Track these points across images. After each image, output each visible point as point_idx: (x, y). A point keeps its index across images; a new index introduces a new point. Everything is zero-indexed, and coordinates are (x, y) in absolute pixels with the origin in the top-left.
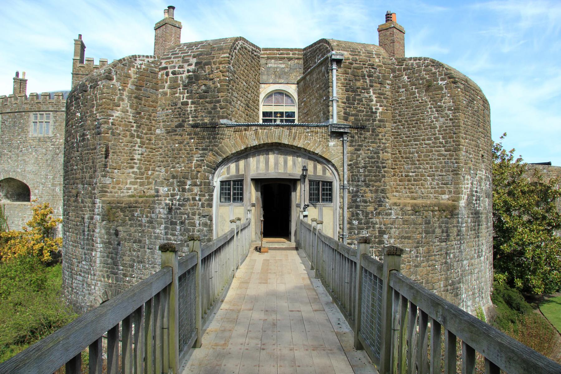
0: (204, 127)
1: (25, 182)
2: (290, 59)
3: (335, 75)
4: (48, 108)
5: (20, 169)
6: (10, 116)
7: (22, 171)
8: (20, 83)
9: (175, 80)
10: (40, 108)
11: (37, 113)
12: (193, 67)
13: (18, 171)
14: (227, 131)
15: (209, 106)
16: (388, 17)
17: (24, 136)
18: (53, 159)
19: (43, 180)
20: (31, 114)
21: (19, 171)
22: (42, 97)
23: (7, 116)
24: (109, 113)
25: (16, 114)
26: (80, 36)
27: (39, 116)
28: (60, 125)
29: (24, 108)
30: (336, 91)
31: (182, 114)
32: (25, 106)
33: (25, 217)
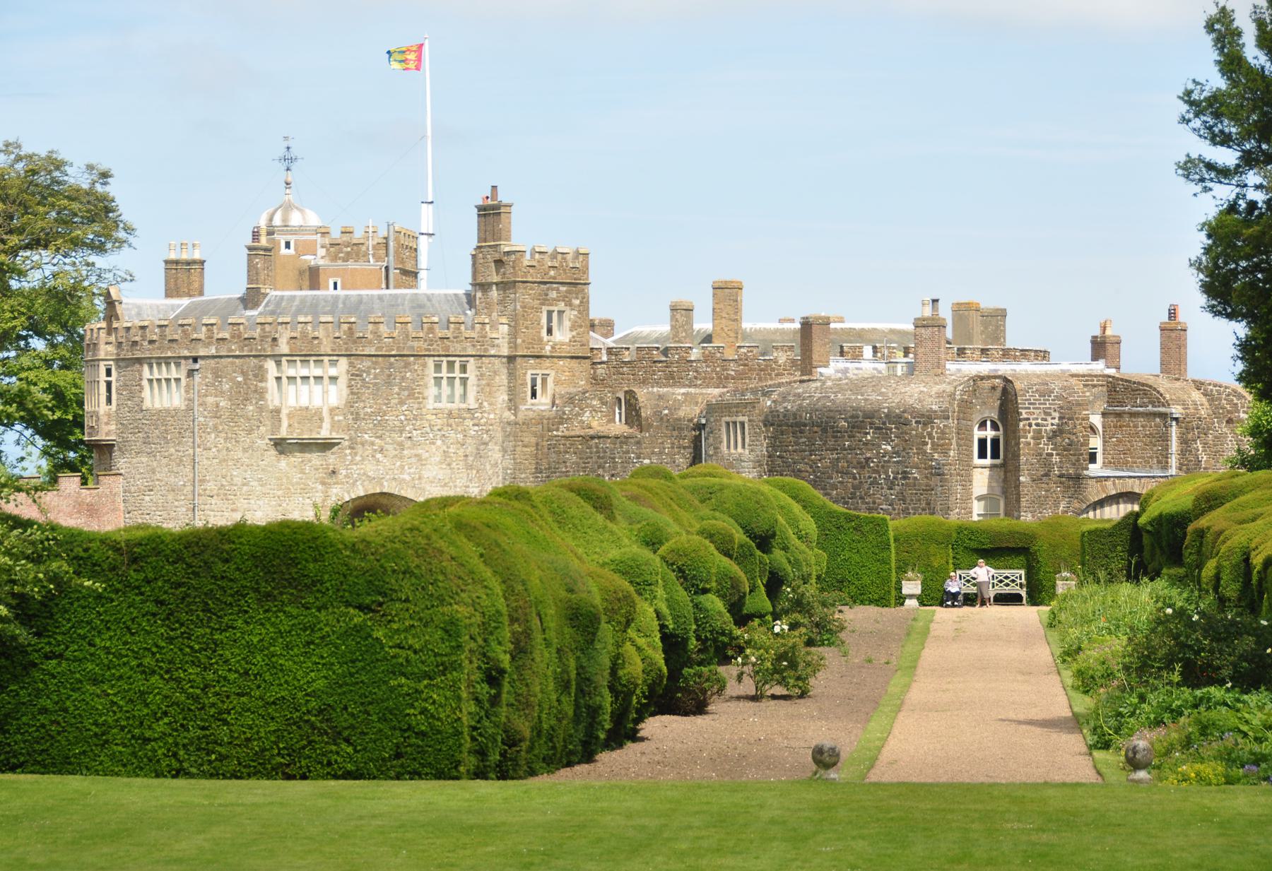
0: (1069, 477)
2: (1094, 386)
3: (1174, 431)
4: (464, 349)
9: (1039, 432)
10: (447, 349)
12: (1056, 421)
13: (404, 480)
14: (1090, 482)
15: (1073, 458)
16: (1172, 313)
17: (416, 406)
18: (478, 455)
20: (430, 362)
21: (407, 477)
23: (367, 363)
25: (392, 359)
26: (494, 188)
27: (444, 365)
28: (488, 385)
30: (1174, 446)
31: (1046, 462)
32: (416, 344)
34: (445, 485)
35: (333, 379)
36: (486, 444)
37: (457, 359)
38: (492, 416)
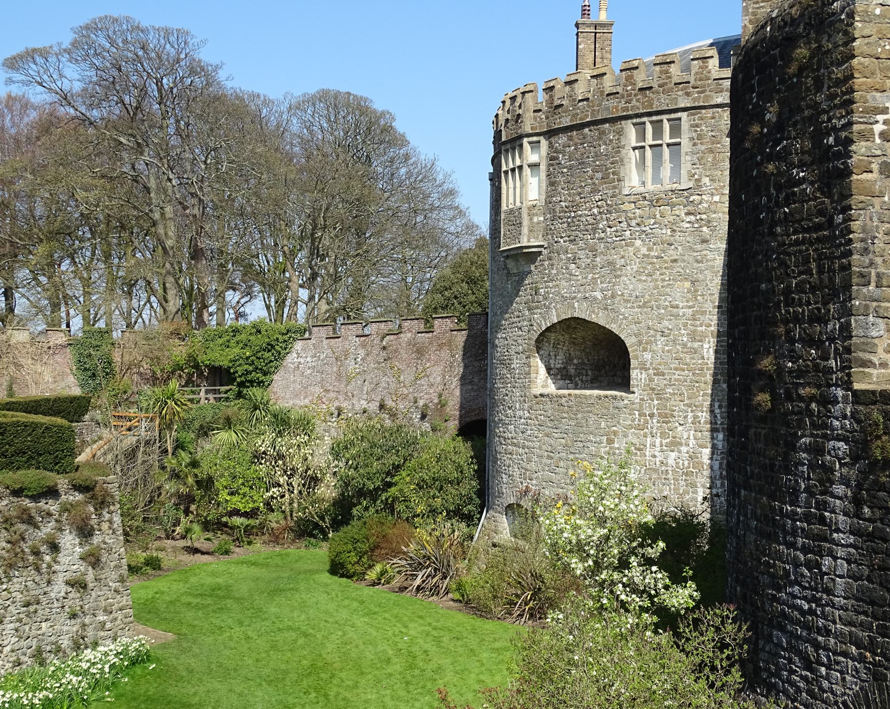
1: (614, 328)
5: (602, 291)
6: (570, 138)
7: (605, 298)
8: (593, 32)
11: (645, 119)
13: (595, 299)
19: (666, 323)
21: (598, 295)
22: (658, 68)
23: (562, 139)
24: (871, 104)
29: (607, 109)
32: (612, 103)
33: (615, 433)
34: (644, 305)
35: (534, 166)
36: (704, 241)
37: (664, 117)
38: (716, 198)
